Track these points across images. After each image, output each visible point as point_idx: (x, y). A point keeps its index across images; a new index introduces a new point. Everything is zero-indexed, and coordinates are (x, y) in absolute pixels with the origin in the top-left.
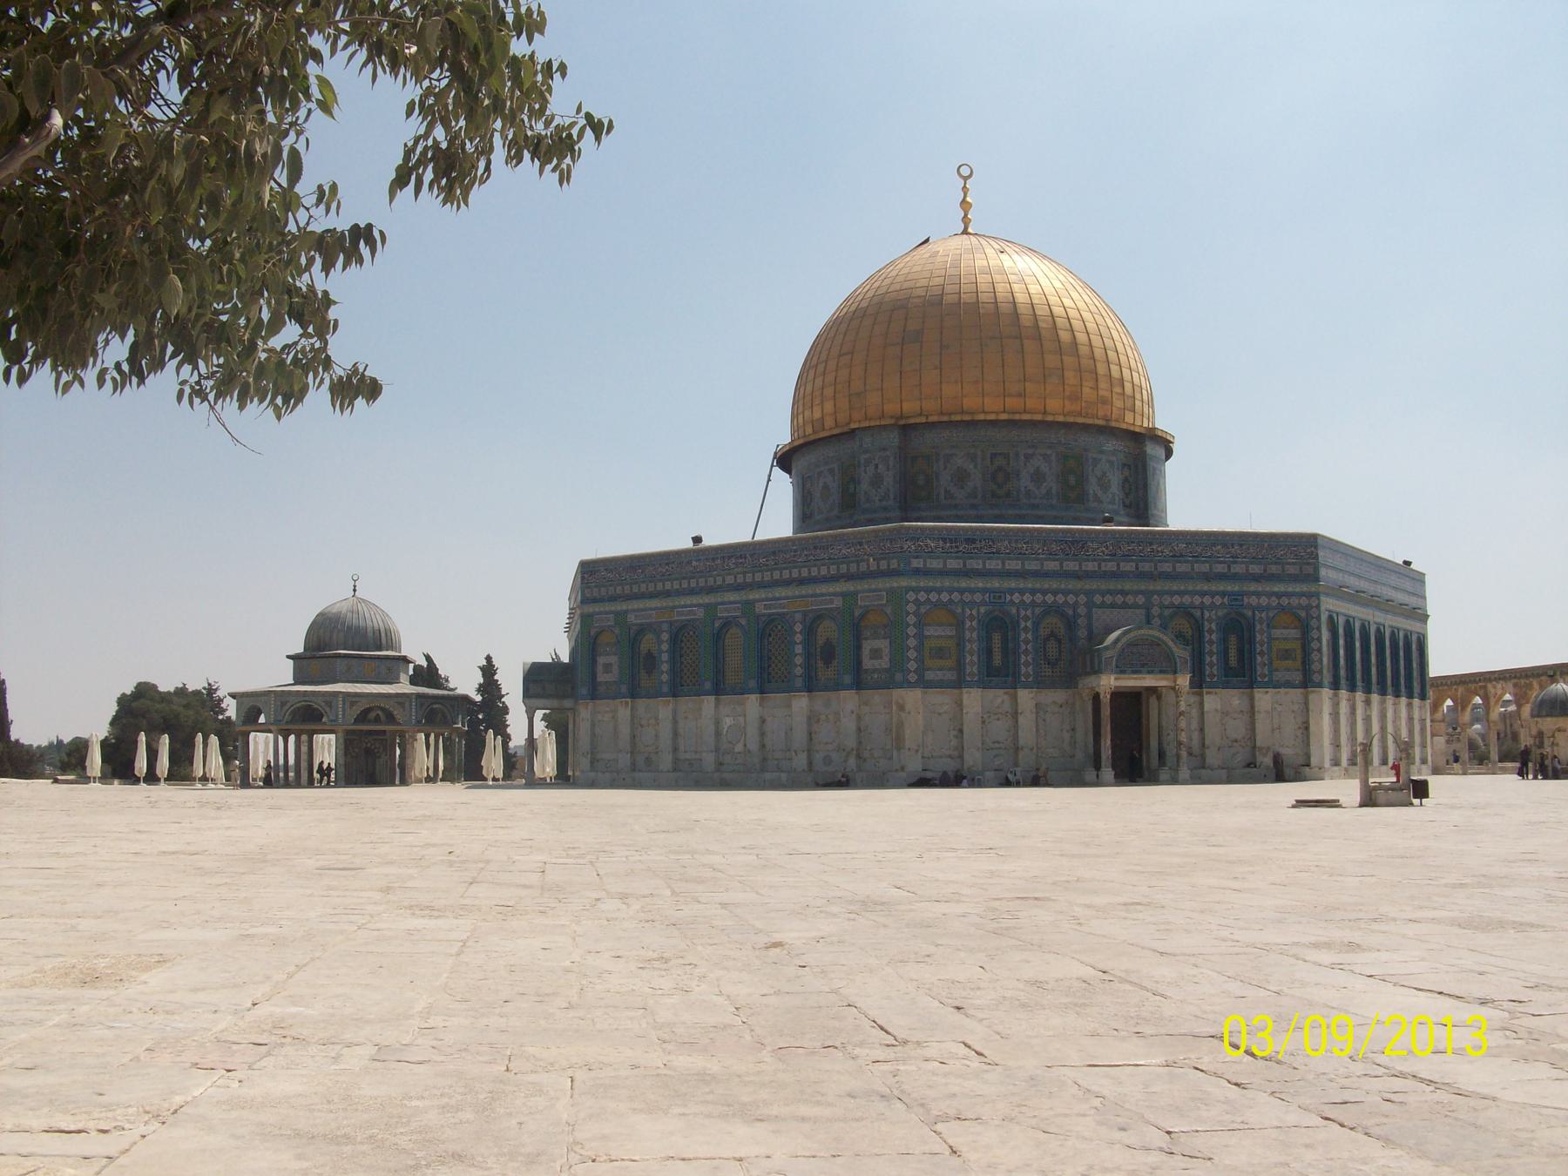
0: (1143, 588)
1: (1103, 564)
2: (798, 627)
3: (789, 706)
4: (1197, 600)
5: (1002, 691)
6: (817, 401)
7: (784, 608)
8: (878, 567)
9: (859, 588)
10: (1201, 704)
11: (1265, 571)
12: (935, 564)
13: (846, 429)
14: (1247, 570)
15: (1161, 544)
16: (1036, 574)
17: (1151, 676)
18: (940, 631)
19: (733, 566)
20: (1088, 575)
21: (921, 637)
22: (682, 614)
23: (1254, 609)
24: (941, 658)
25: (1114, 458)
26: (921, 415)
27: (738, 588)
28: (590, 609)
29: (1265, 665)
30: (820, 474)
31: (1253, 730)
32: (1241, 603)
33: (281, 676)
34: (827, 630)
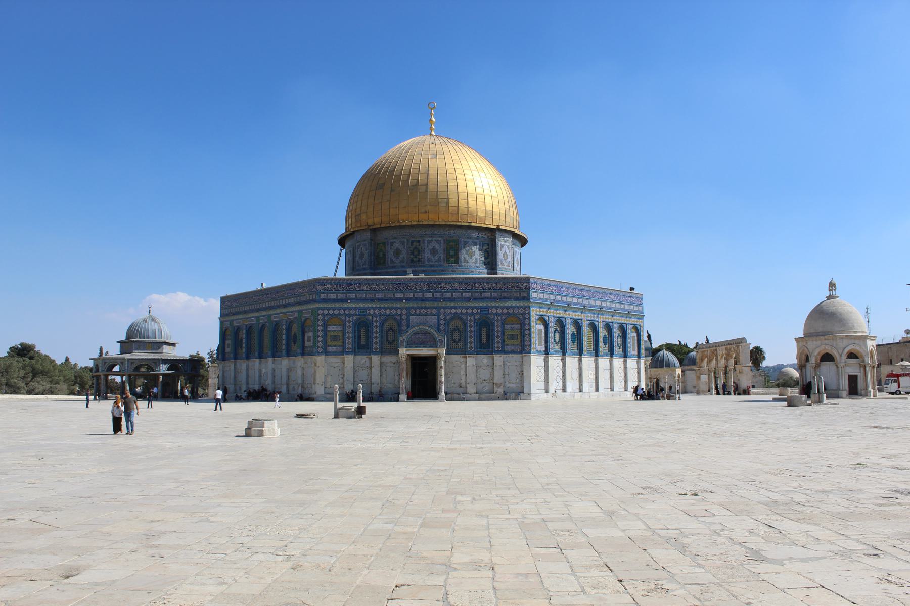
0: (436, 305)
1: (416, 294)
2: (284, 327)
3: (281, 364)
4: (464, 311)
10: (466, 362)
12: (332, 296)
14: (491, 295)
16: (380, 300)
18: (335, 328)
20: (408, 300)
21: (325, 332)
22: (250, 321)
27: (265, 309)
29: (499, 342)
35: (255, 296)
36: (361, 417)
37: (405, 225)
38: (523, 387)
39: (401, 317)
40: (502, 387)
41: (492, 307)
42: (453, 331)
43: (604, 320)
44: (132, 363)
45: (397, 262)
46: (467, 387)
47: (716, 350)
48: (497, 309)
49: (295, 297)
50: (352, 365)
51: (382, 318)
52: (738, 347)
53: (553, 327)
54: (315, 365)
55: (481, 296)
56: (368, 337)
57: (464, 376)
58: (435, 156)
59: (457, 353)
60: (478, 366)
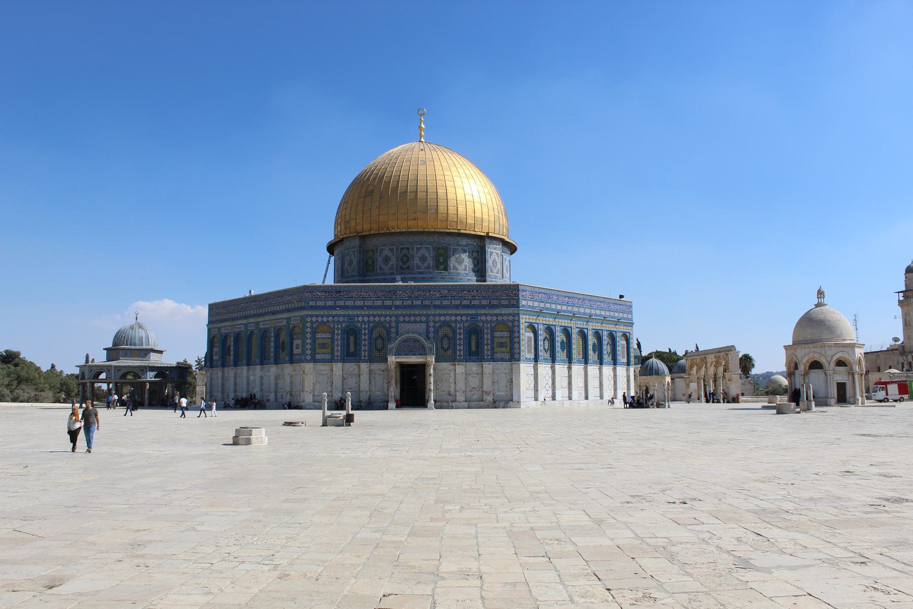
0: (425, 313)
1: (404, 302)
2: (272, 334)
3: (269, 371)
4: (453, 318)
5: (354, 364)
11: (490, 303)
12: (321, 303)
16: (369, 307)
17: (415, 356)
18: (323, 335)
20: (397, 307)
21: (314, 339)
22: (237, 328)
23: (483, 322)
24: (323, 348)
27: (254, 316)
29: (489, 350)
32: (477, 319)
35: (243, 303)
36: (350, 425)
37: (395, 232)
38: (512, 395)
41: (481, 315)
42: (442, 339)
43: (594, 327)
44: (119, 370)
45: (386, 268)
46: (456, 395)
47: (705, 358)
48: (486, 316)
49: (284, 304)
51: (370, 326)
52: (727, 355)
53: (542, 335)
54: (304, 372)
56: (356, 345)
57: (453, 384)
58: (425, 163)
59: (446, 361)
60: (467, 374)
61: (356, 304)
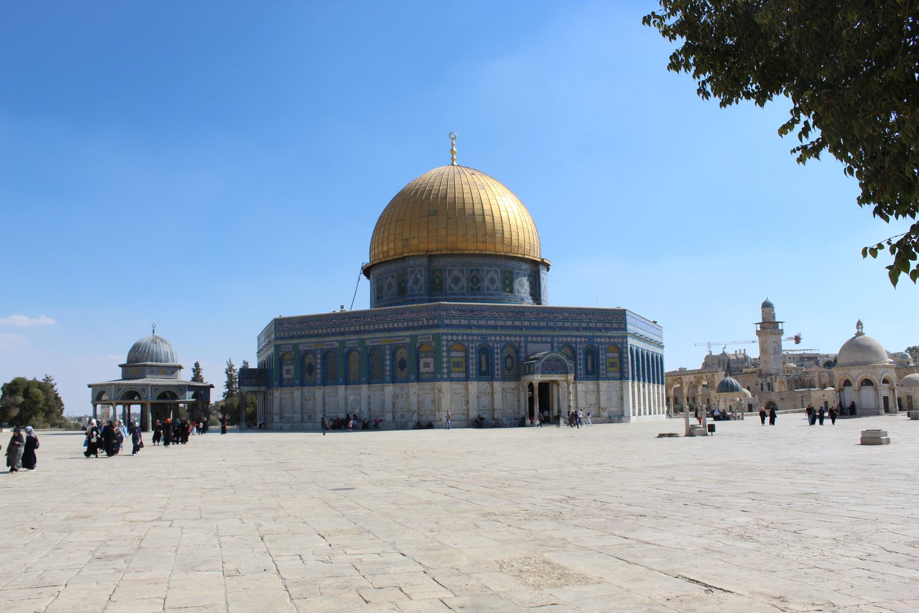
1: (532, 322)
2: (388, 352)
3: (383, 390)
4: (574, 339)
6: (385, 242)
7: (380, 342)
8: (428, 323)
9: (419, 333)
10: (576, 388)
11: (604, 326)
12: (455, 322)
13: (401, 256)
15: (557, 314)
17: (557, 375)
18: (458, 354)
19: (354, 322)
21: (448, 356)
22: (326, 345)
24: (457, 367)
25: (525, 273)
26: (437, 250)
28: (279, 342)
29: (604, 369)
30: (386, 278)
31: (599, 400)
33: (114, 375)
34: (402, 354)
35: (335, 319)
39: (519, 344)
40: (607, 411)
41: (597, 337)
45: (456, 289)
50: (476, 391)
55: (588, 325)
61: (489, 324)
